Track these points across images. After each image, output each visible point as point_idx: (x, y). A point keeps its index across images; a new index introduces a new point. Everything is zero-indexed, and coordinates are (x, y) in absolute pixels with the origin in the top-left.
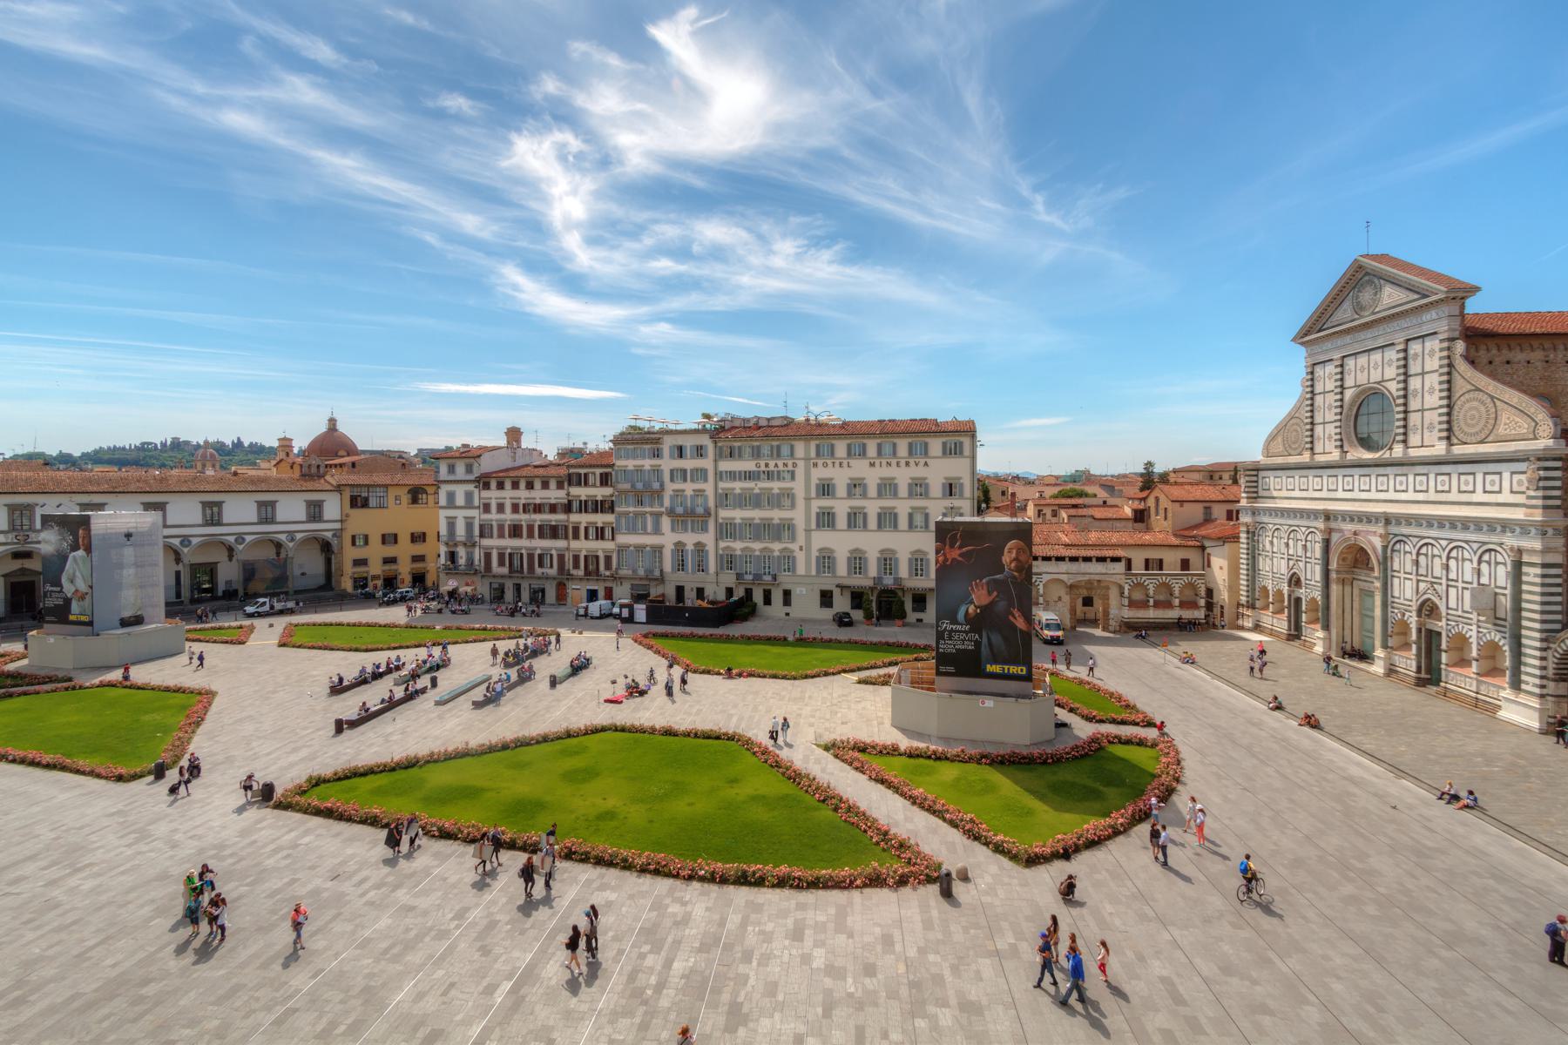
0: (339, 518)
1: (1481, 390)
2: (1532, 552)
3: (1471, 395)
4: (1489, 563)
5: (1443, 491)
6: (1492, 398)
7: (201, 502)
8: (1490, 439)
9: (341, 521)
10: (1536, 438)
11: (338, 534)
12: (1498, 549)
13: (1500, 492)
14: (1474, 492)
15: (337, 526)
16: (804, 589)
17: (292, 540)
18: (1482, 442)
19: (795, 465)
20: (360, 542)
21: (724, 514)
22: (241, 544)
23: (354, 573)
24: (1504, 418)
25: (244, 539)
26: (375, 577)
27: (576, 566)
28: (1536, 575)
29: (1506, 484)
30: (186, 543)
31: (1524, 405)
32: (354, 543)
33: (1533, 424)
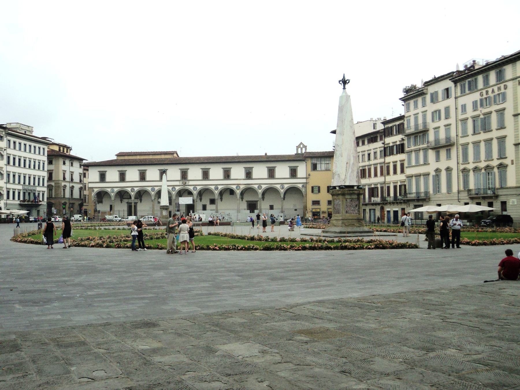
0: (305, 177)
7: (244, 168)
9: (306, 178)
11: (305, 185)
15: (304, 181)
16: (515, 200)
17: (283, 188)
19: (506, 87)
20: (316, 190)
21: (462, 141)
22: (260, 189)
23: (313, 209)
25: (261, 187)
26: (324, 212)
27: (389, 194)
30: (238, 188)
32: (313, 191)
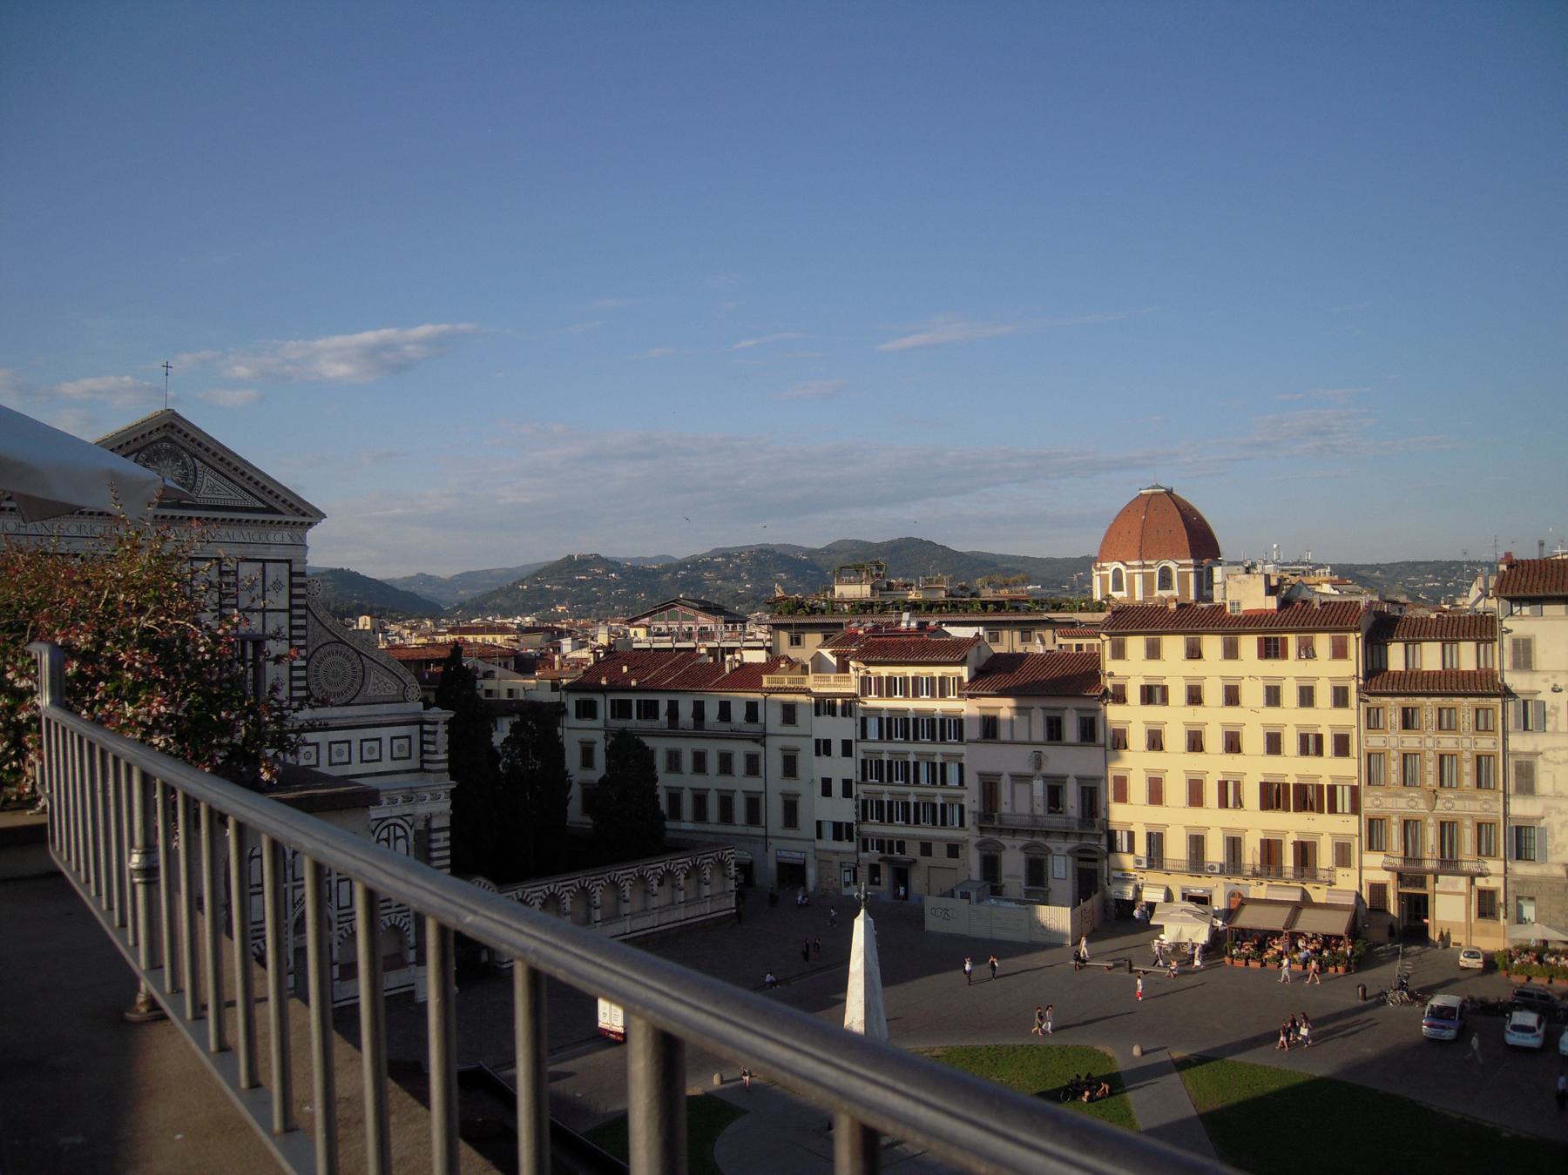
1: (346, 644)
2: (441, 814)
3: (334, 648)
4: (387, 840)
5: (373, 761)
6: (359, 653)
8: (357, 700)
10: (405, 701)
12: (400, 822)
13: (380, 760)
14: (349, 763)
18: (347, 704)
24: (372, 679)
28: (438, 840)
29: (324, 752)
31: (393, 664)
33: (403, 686)
